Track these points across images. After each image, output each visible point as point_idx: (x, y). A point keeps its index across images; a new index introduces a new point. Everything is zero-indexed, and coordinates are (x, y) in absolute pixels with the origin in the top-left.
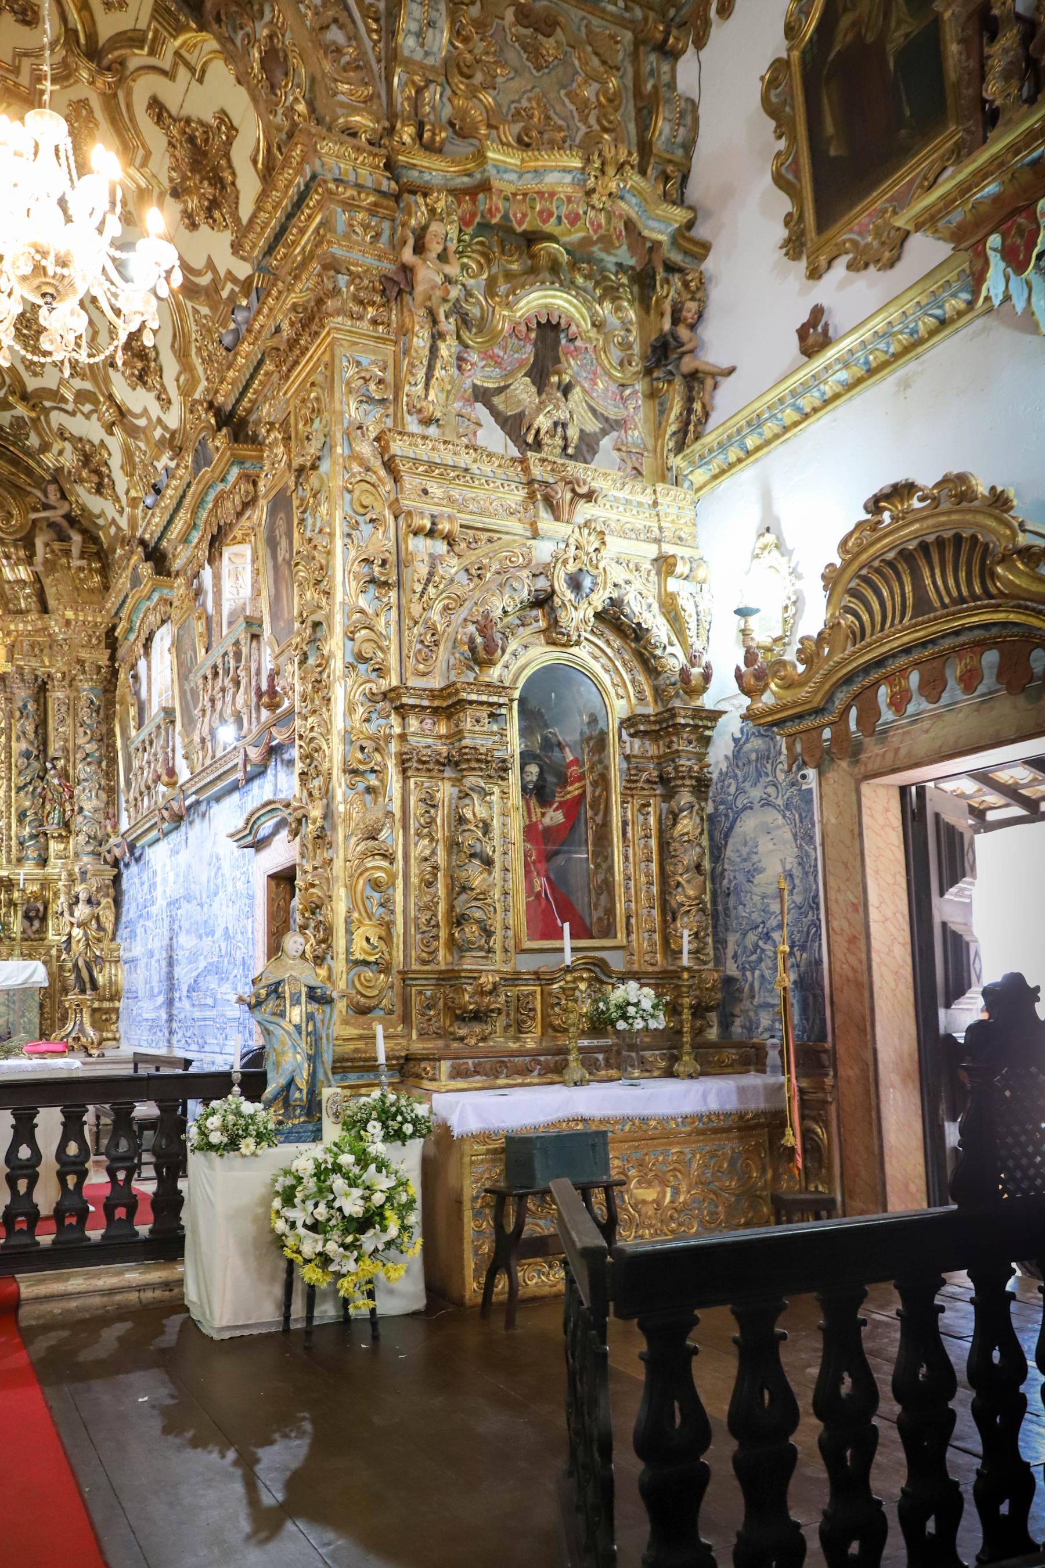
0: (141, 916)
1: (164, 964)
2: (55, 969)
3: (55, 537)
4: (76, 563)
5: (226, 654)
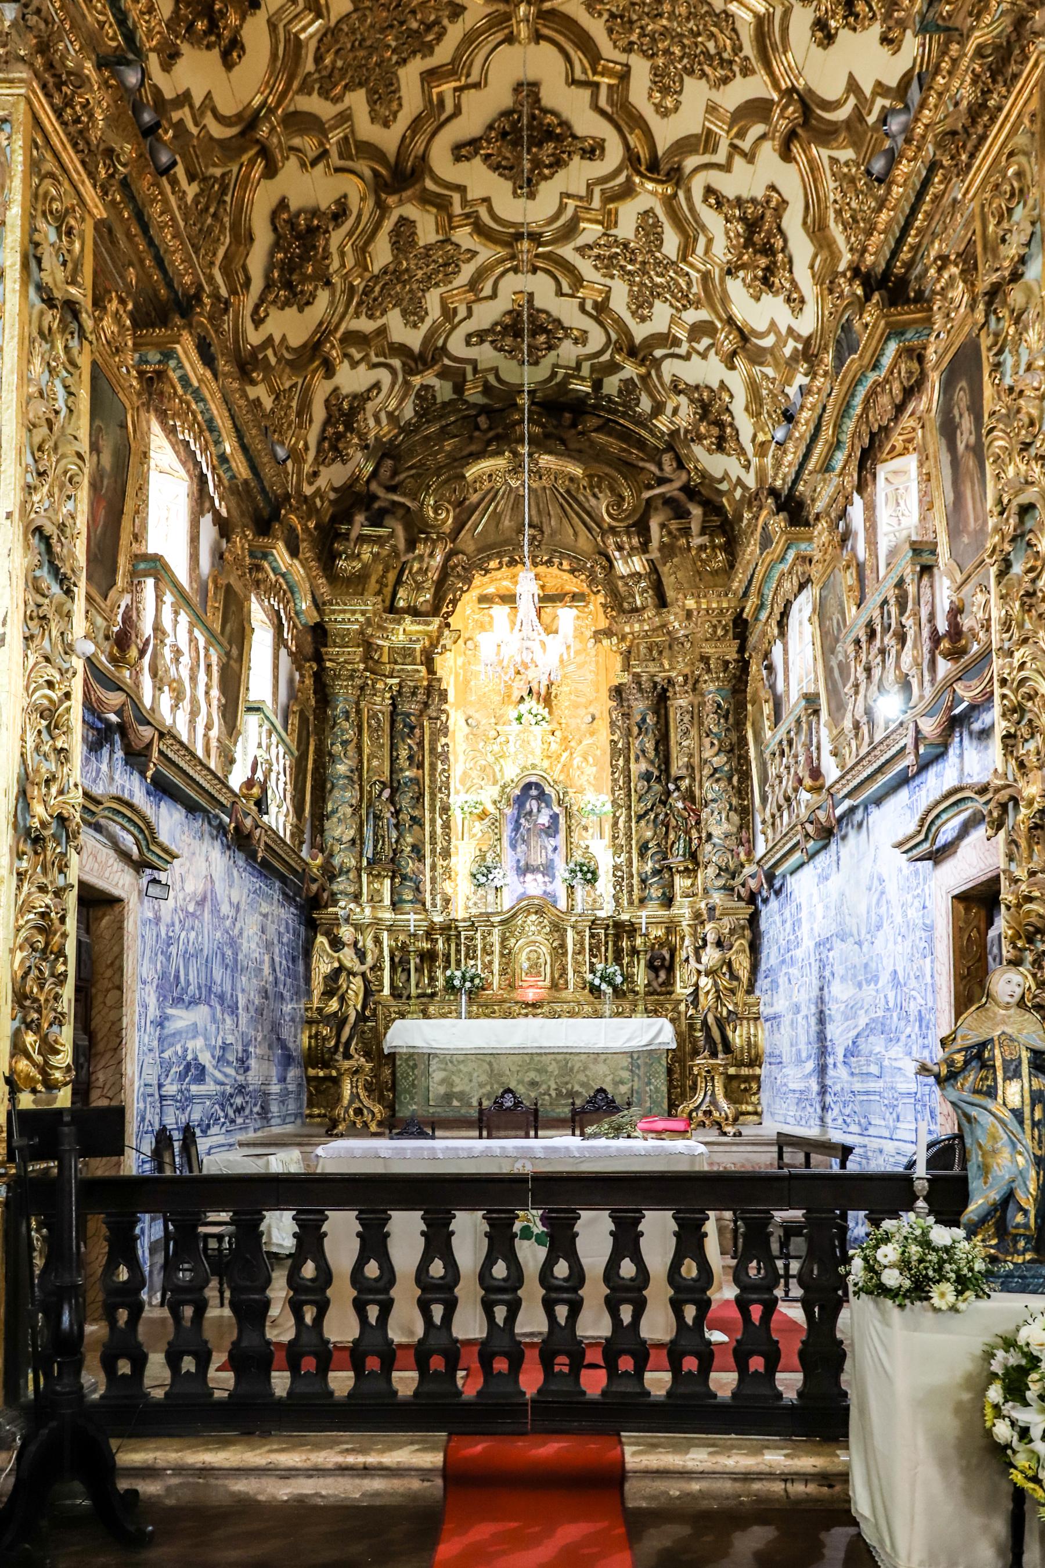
2: (684, 1028)
4: (697, 541)
5: (885, 602)
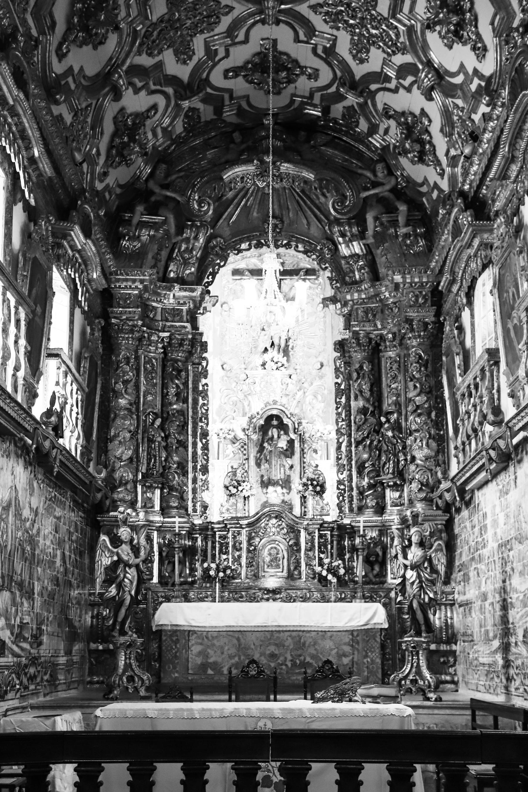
1: (498, 607)
2: (394, 611)
3: (384, 210)
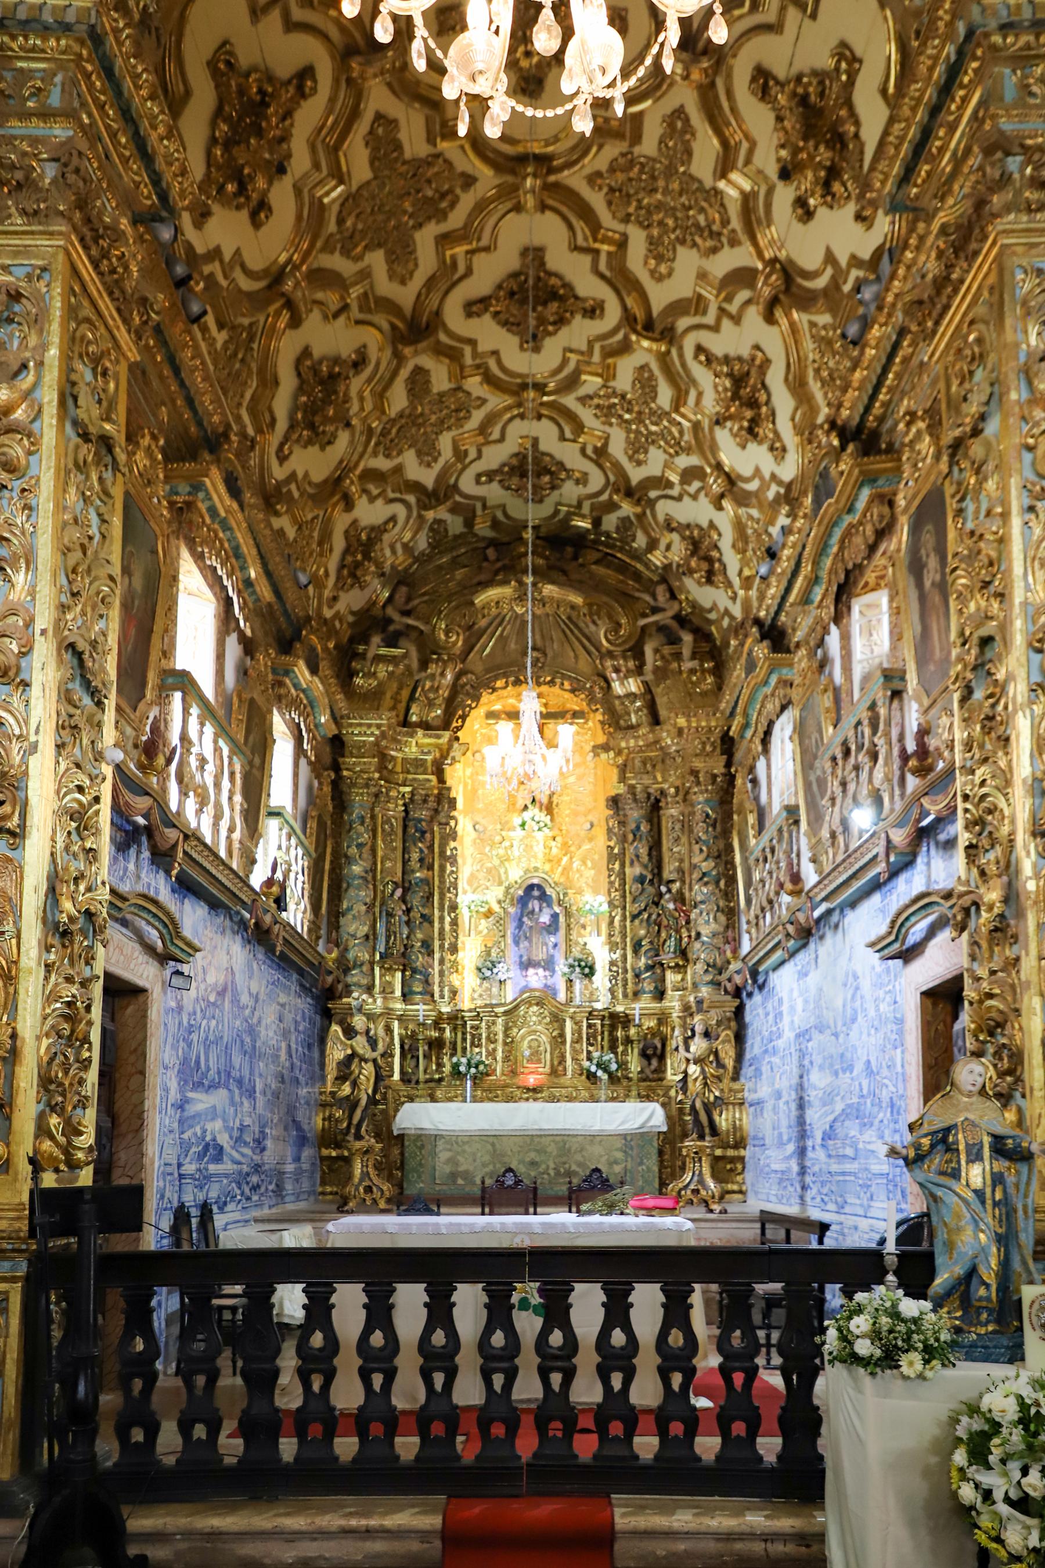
0: (766, 1051)
4: (688, 665)
5: (859, 723)
